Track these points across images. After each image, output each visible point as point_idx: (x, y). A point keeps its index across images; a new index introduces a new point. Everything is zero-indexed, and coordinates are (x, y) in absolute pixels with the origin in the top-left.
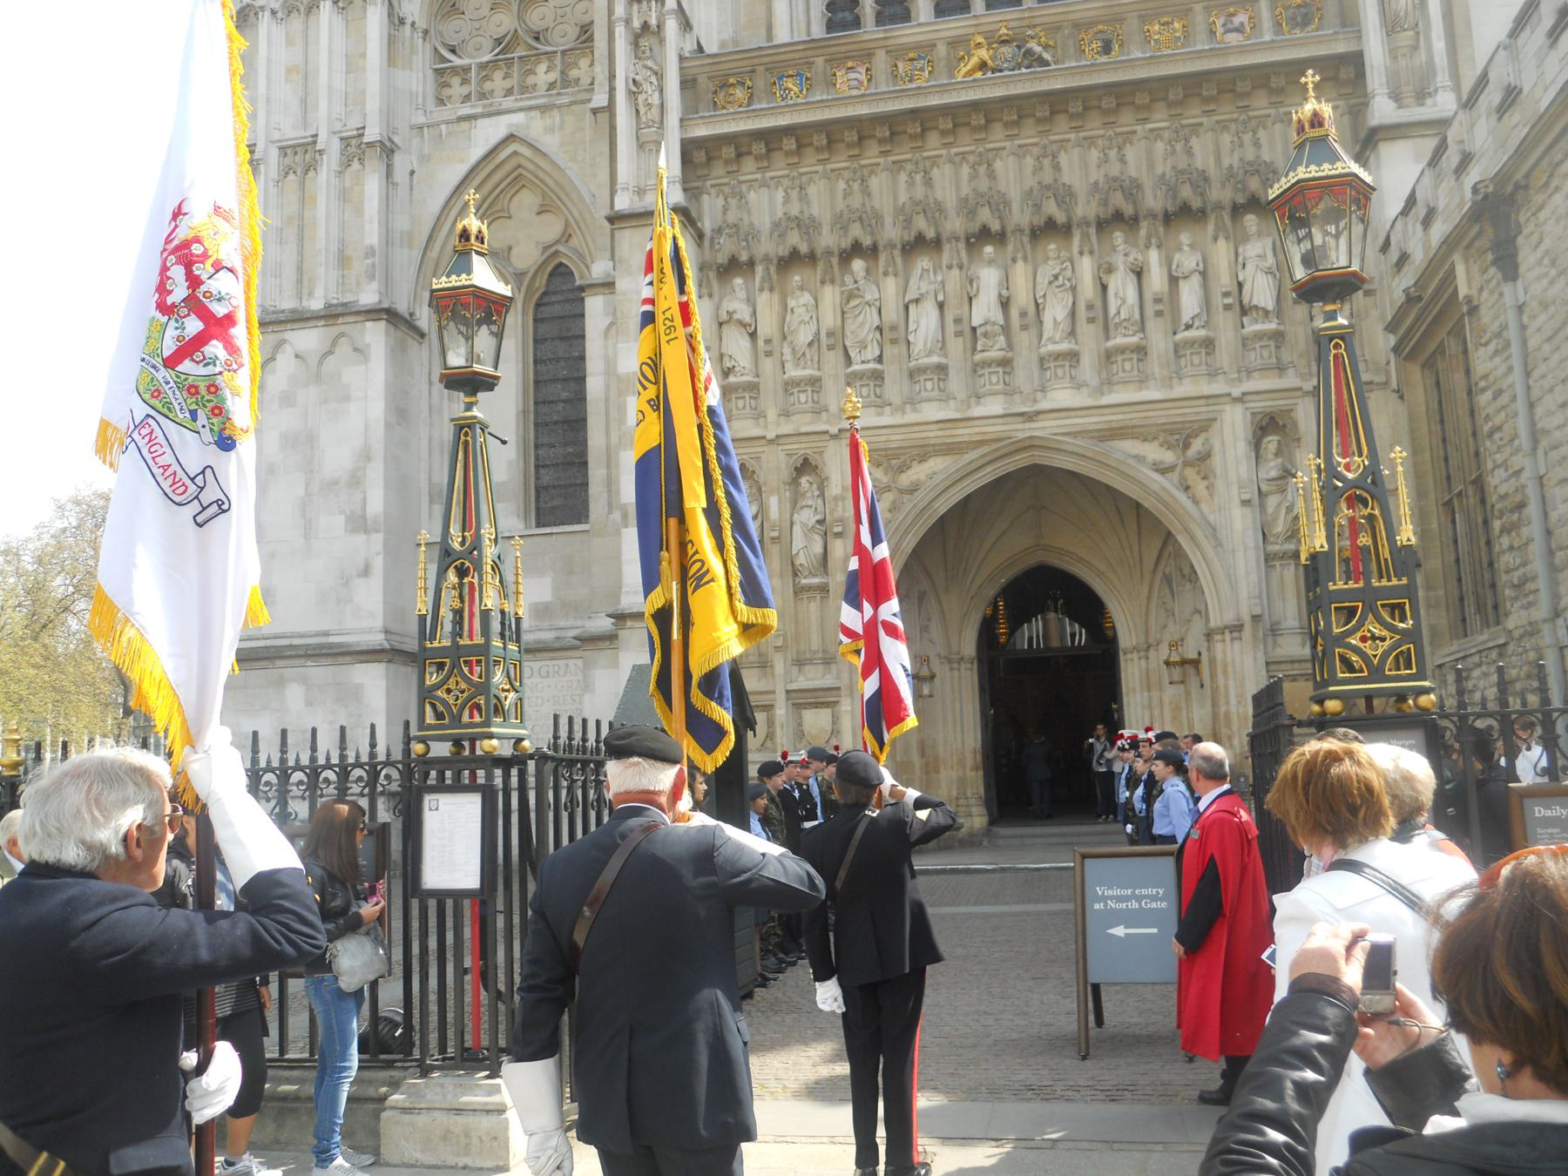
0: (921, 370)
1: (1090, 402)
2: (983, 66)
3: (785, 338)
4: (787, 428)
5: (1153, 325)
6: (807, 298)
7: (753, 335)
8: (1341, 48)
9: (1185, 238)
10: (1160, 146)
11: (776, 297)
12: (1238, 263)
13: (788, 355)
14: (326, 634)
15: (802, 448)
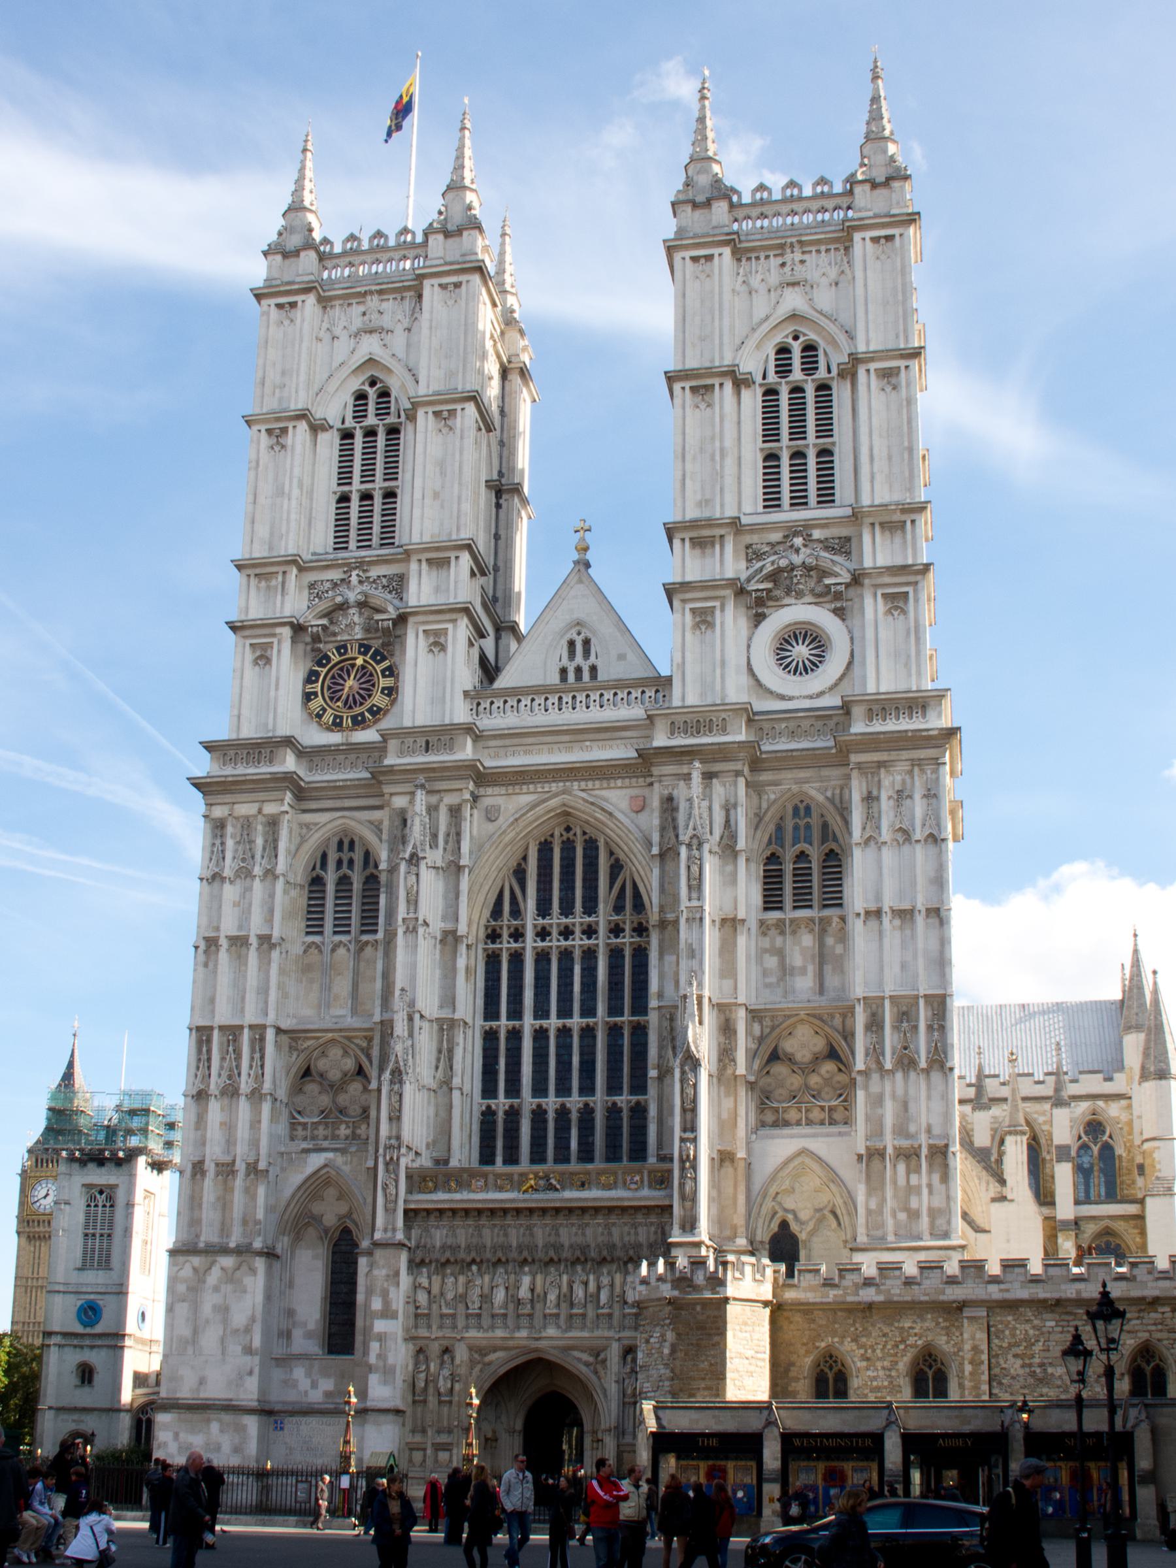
0: (497, 1315)
1: (560, 1335)
2: (532, 1187)
3: (442, 1294)
4: (440, 1334)
5: (589, 1306)
6: (452, 1279)
7: (429, 1292)
8: (667, 1203)
9: (605, 1271)
10: (600, 1229)
11: (439, 1278)
12: (624, 1283)
13: (443, 1304)
14: (231, 1400)
15: (445, 1343)
